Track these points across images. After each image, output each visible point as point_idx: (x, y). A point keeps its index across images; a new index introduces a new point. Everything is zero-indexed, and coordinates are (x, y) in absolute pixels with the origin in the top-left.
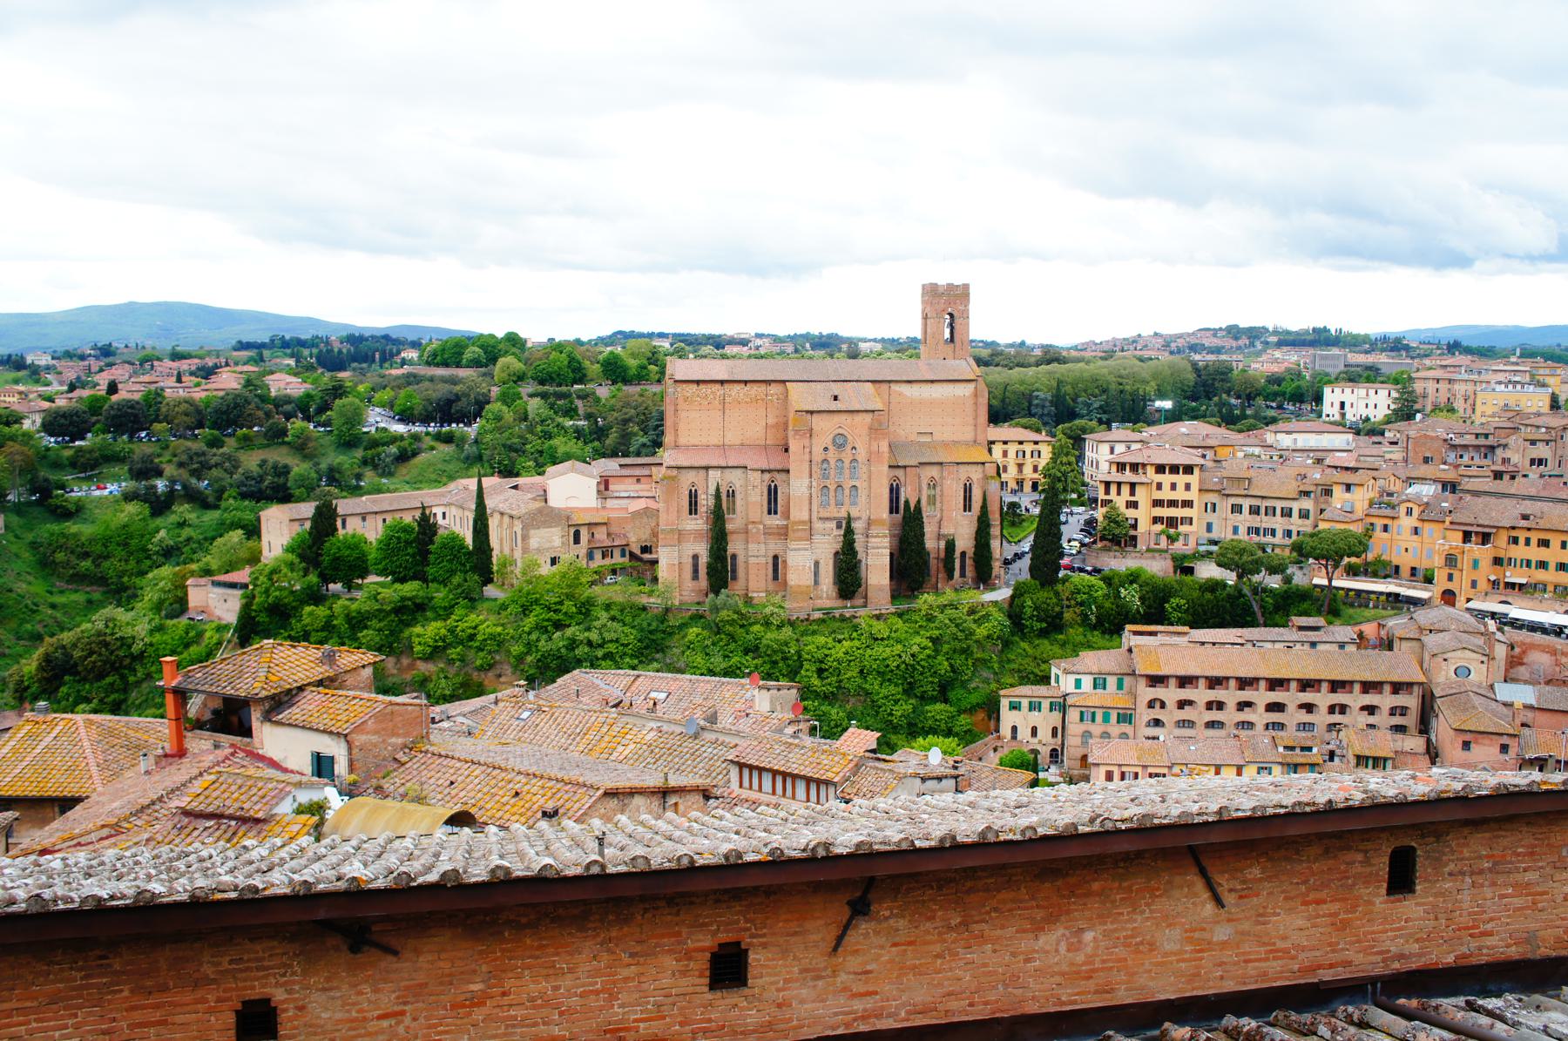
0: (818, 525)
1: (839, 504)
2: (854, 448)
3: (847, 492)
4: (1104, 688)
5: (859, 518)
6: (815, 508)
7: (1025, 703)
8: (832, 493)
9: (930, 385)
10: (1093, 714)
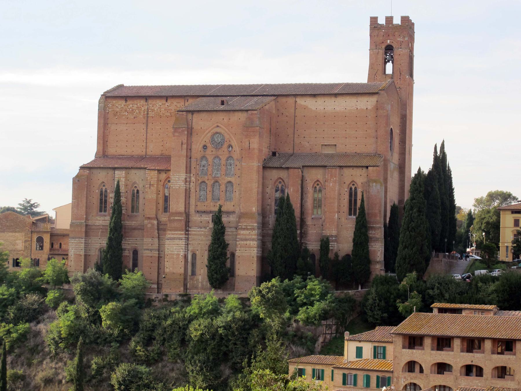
0: (195, 218)
1: (215, 199)
4: (384, 357)
5: (234, 212)
6: (193, 201)
7: (309, 369)
9: (333, 99)
10: (355, 376)
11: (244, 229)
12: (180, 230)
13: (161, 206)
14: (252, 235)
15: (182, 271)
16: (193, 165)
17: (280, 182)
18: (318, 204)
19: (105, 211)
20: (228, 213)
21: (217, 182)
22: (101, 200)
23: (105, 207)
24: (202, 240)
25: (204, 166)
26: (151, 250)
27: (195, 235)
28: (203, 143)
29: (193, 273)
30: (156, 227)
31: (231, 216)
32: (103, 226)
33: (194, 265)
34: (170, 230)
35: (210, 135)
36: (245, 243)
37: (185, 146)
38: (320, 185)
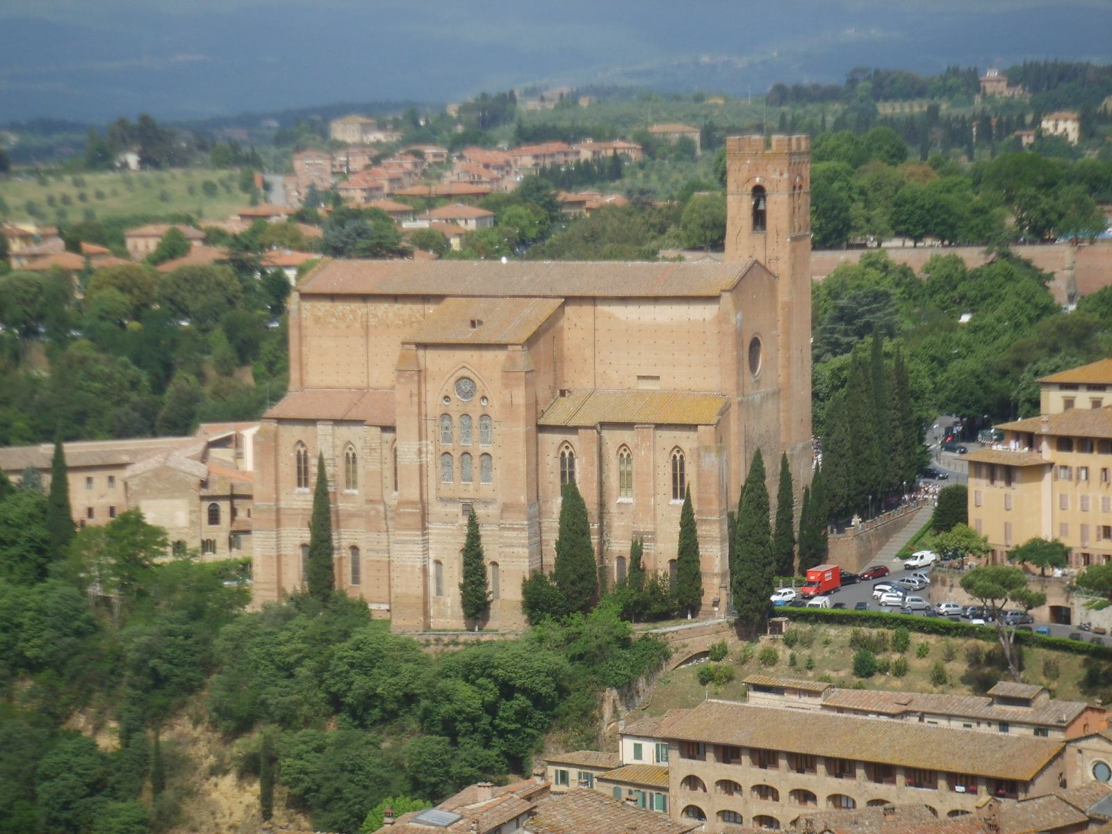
0: (436, 508)
2: (484, 398)
3: (476, 461)
6: (431, 482)
8: (456, 464)
11: (509, 529)
12: (414, 529)
13: (389, 481)
14: (521, 538)
15: (420, 591)
16: (431, 426)
17: (567, 447)
18: (626, 481)
19: (306, 485)
20: (486, 503)
21: (466, 453)
22: (299, 468)
23: (306, 480)
24: (450, 543)
25: (447, 428)
26: (378, 551)
27: (438, 534)
28: (444, 393)
29: (439, 592)
30: (383, 516)
31: (490, 507)
32: (304, 509)
33: (439, 579)
34: (400, 529)
35: (453, 380)
36: (511, 550)
37: (415, 399)
38: (628, 452)
